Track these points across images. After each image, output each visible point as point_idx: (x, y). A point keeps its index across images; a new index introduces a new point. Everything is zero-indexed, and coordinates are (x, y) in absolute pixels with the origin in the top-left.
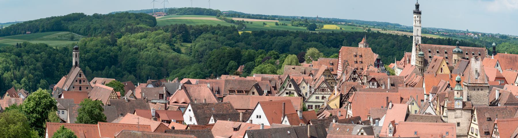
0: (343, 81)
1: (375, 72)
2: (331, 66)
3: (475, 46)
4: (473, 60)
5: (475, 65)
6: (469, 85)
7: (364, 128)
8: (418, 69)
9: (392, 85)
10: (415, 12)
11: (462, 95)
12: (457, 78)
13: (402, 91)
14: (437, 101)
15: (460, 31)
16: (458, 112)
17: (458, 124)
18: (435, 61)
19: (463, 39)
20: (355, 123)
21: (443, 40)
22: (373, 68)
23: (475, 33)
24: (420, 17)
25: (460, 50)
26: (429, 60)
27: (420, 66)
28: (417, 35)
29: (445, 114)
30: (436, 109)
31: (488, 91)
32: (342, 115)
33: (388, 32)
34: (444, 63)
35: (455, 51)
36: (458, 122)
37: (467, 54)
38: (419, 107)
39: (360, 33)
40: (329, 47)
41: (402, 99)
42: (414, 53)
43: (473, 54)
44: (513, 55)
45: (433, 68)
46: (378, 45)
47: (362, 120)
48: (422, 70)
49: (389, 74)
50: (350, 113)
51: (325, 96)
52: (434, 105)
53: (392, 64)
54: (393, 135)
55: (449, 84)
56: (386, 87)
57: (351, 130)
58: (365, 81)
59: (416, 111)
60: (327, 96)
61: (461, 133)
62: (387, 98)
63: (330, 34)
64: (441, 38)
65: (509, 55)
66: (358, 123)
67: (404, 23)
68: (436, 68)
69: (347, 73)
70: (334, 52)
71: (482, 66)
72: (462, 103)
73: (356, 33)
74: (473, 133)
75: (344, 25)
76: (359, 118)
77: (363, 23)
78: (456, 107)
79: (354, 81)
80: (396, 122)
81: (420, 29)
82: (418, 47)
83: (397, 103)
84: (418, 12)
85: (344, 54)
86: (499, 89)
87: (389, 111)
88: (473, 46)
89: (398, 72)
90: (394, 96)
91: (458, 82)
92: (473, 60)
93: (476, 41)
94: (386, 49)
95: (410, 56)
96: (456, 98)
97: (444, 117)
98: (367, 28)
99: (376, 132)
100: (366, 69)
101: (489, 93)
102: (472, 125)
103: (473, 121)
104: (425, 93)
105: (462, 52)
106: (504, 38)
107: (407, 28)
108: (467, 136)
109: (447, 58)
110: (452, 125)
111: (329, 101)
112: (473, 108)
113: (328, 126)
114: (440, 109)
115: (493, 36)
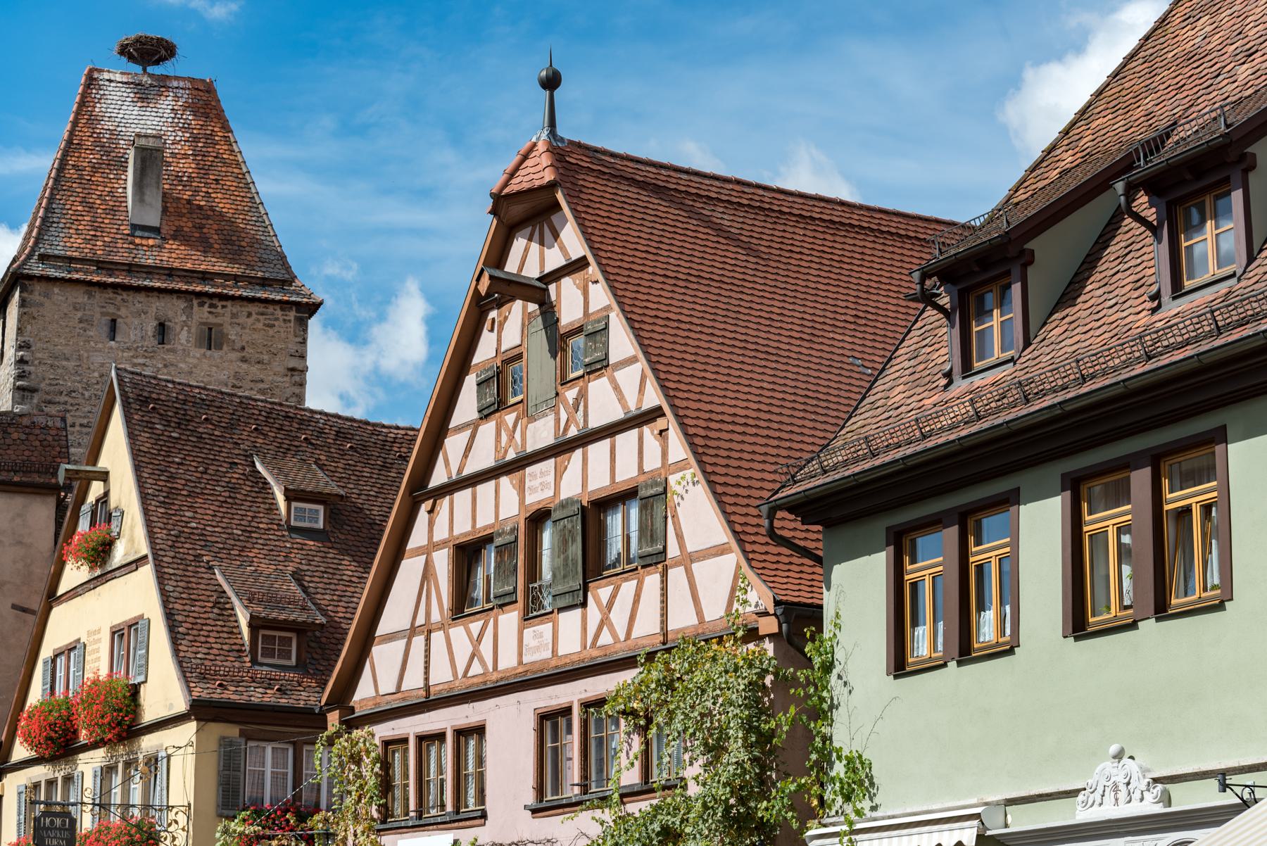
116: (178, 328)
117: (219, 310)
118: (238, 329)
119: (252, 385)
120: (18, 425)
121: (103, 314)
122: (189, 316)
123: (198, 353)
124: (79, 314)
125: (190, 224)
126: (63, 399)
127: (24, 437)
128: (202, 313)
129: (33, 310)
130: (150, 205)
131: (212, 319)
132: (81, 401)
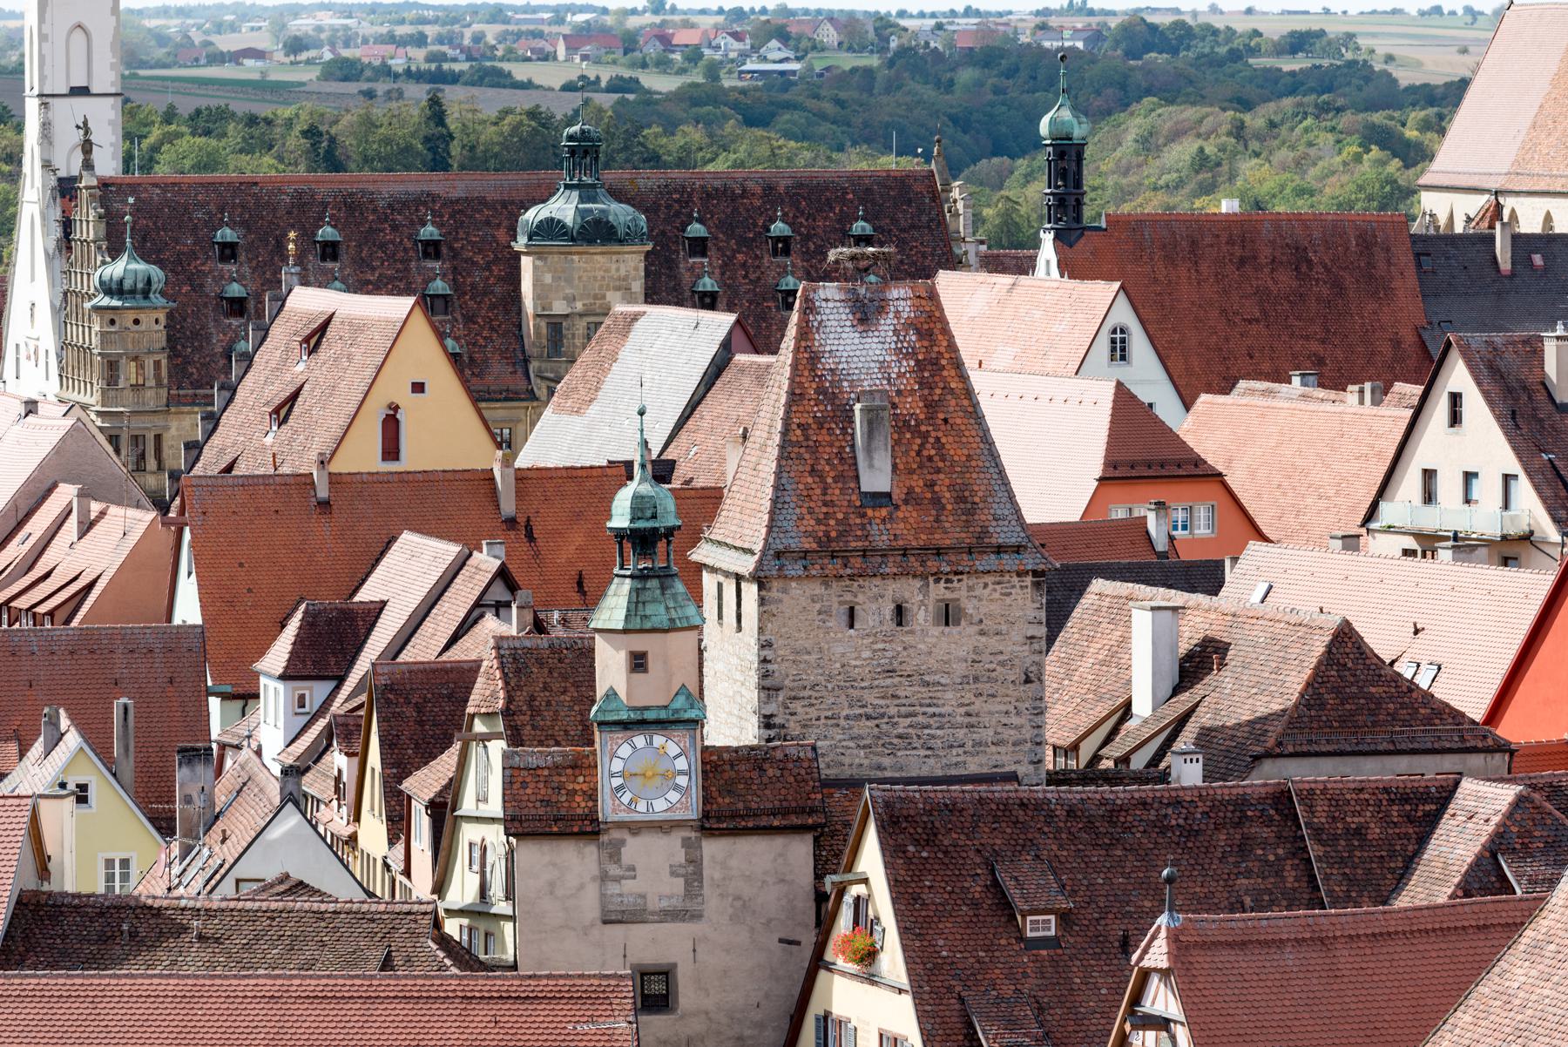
18: (315, 338)
116: (915, 608)
117: (955, 584)
118: (975, 601)
119: (992, 658)
120: (772, 760)
121: (840, 603)
122: (926, 595)
123: (936, 631)
124: (818, 606)
125: (921, 483)
126: (806, 693)
127: (778, 773)
128: (938, 591)
129: (773, 608)
130: (880, 470)
131: (949, 595)
132: (825, 693)
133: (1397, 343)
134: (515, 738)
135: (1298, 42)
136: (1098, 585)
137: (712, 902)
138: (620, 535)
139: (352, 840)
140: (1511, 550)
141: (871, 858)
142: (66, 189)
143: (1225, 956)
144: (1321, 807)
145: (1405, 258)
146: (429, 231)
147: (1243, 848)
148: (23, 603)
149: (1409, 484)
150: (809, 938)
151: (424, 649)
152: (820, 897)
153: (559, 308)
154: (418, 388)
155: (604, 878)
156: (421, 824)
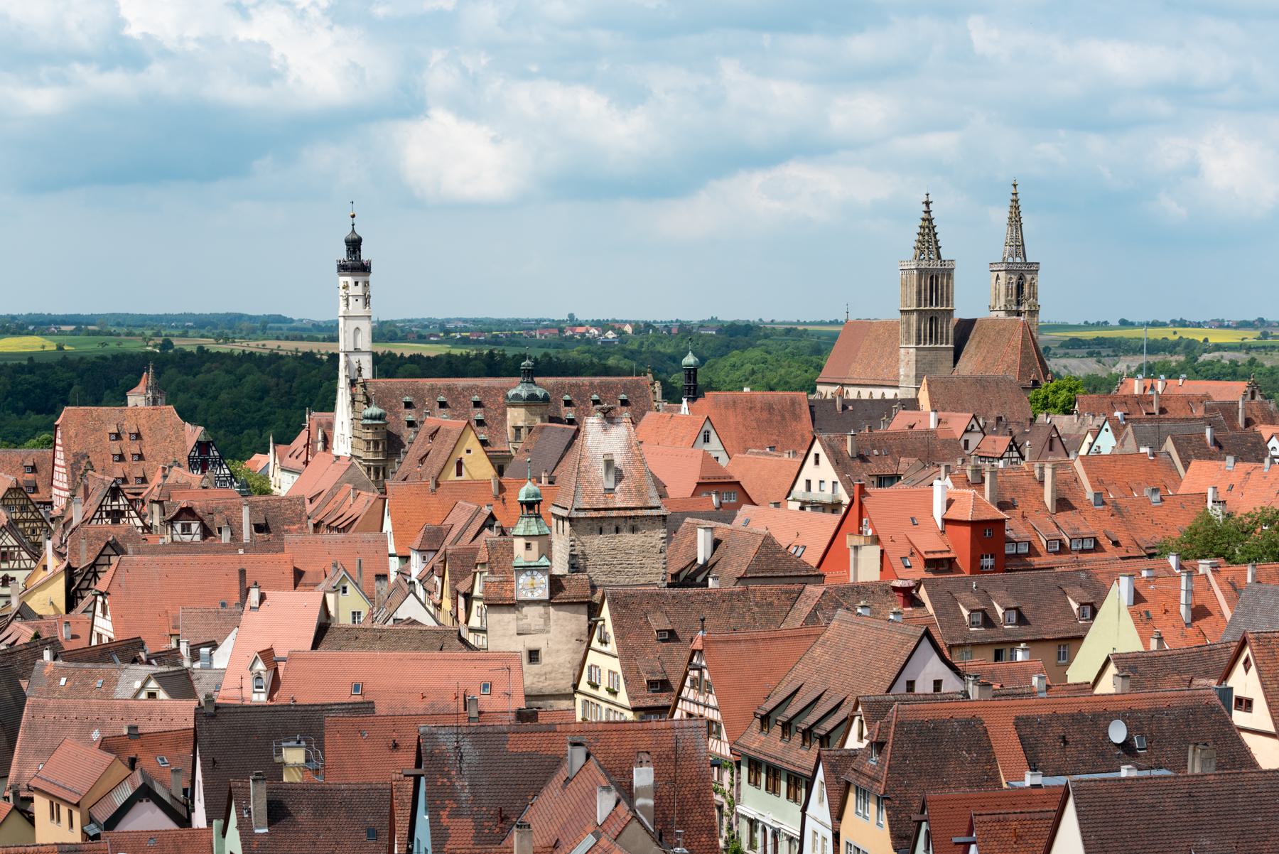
0: (74, 524)
1: (192, 486)
2: (30, 477)
3: (607, 371)
4: (593, 424)
5: (603, 440)
6: (575, 514)
7: (158, 677)
8: (363, 470)
9: (260, 528)
10: (343, 268)
11: (547, 551)
12: (526, 491)
13: (299, 546)
14: (443, 577)
15: (538, 322)
16: (532, 615)
17: (534, 656)
18: (433, 435)
19: (552, 352)
20: (123, 661)
21: (466, 359)
22: (181, 475)
23: (603, 325)
24: (366, 284)
25: (539, 392)
26: (407, 434)
27: (370, 456)
28: (354, 347)
29: (475, 622)
30: (438, 606)
31: (661, 533)
32: (74, 637)
33: (238, 347)
34: (471, 441)
35: (517, 396)
36: (533, 646)
37: (568, 403)
38: (370, 599)
39: (132, 357)
40: (20, 412)
41: (298, 574)
42: (343, 413)
43: (596, 402)
44: (779, 393)
45: (422, 460)
46: (202, 396)
47: (150, 648)
48: (380, 471)
49: (247, 489)
50: (105, 627)
51: (11, 574)
52: (428, 592)
53: (257, 457)
54: (270, 697)
55: (492, 517)
56: (236, 536)
57: (111, 682)
58: (156, 521)
59: (356, 615)
60: (20, 576)
61: (547, 686)
62: (242, 573)
63: (19, 369)
64: (457, 351)
65: (762, 395)
66: (135, 661)
67: (302, 307)
68: (435, 462)
69: (87, 496)
70: (37, 430)
71: (635, 447)
72: (543, 580)
73: (118, 358)
74: (595, 687)
75: (73, 333)
76: (138, 644)
77: (143, 321)
78: (523, 595)
79: (116, 521)
80: (280, 653)
81: (366, 327)
82: (359, 390)
83: (279, 588)
84: (355, 264)
85: (72, 432)
86: (713, 524)
87: (248, 618)
88: (595, 375)
89: (283, 484)
90: (260, 564)
91: (530, 505)
92: (593, 424)
93: (609, 354)
94: (235, 405)
95: (330, 425)
96: (520, 561)
97: (471, 630)
98: (159, 341)
99: (202, 688)
100: (156, 479)
101: (668, 539)
102: (592, 658)
103: (595, 643)
104: (392, 550)
105: (546, 399)
106: (738, 335)
107: (317, 327)
108: (570, 697)
109: (480, 423)
110: (506, 661)
111: (28, 591)
112: (597, 598)
113: (27, 674)
114: (455, 604)
115: (685, 330)
133: (803, 436)
134: (492, 572)
135: (788, 332)
136: (688, 520)
137: (553, 627)
138: (522, 503)
139: (440, 605)
140: (834, 507)
141: (605, 612)
142: (353, 383)
143: (720, 645)
144: (758, 594)
145: (806, 407)
146: (476, 398)
147: (732, 609)
148: (334, 525)
149: (801, 485)
150: (585, 639)
151: (465, 541)
152: (590, 626)
153: (520, 424)
154: (469, 451)
155: (517, 619)
156: (461, 600)
